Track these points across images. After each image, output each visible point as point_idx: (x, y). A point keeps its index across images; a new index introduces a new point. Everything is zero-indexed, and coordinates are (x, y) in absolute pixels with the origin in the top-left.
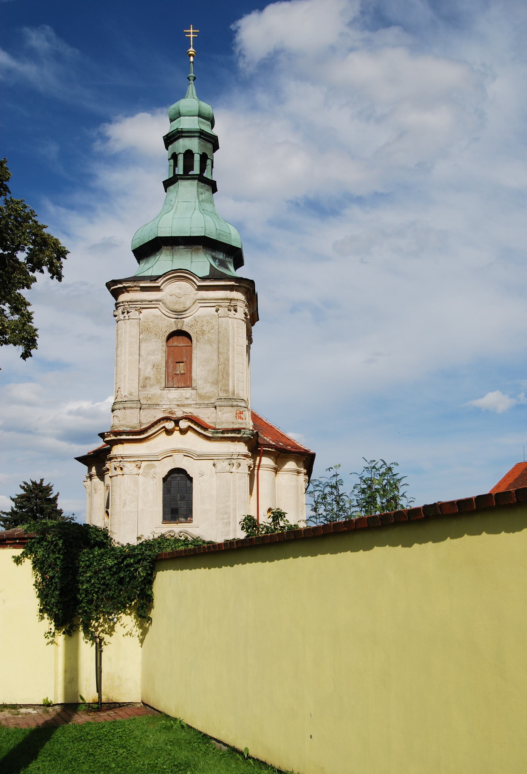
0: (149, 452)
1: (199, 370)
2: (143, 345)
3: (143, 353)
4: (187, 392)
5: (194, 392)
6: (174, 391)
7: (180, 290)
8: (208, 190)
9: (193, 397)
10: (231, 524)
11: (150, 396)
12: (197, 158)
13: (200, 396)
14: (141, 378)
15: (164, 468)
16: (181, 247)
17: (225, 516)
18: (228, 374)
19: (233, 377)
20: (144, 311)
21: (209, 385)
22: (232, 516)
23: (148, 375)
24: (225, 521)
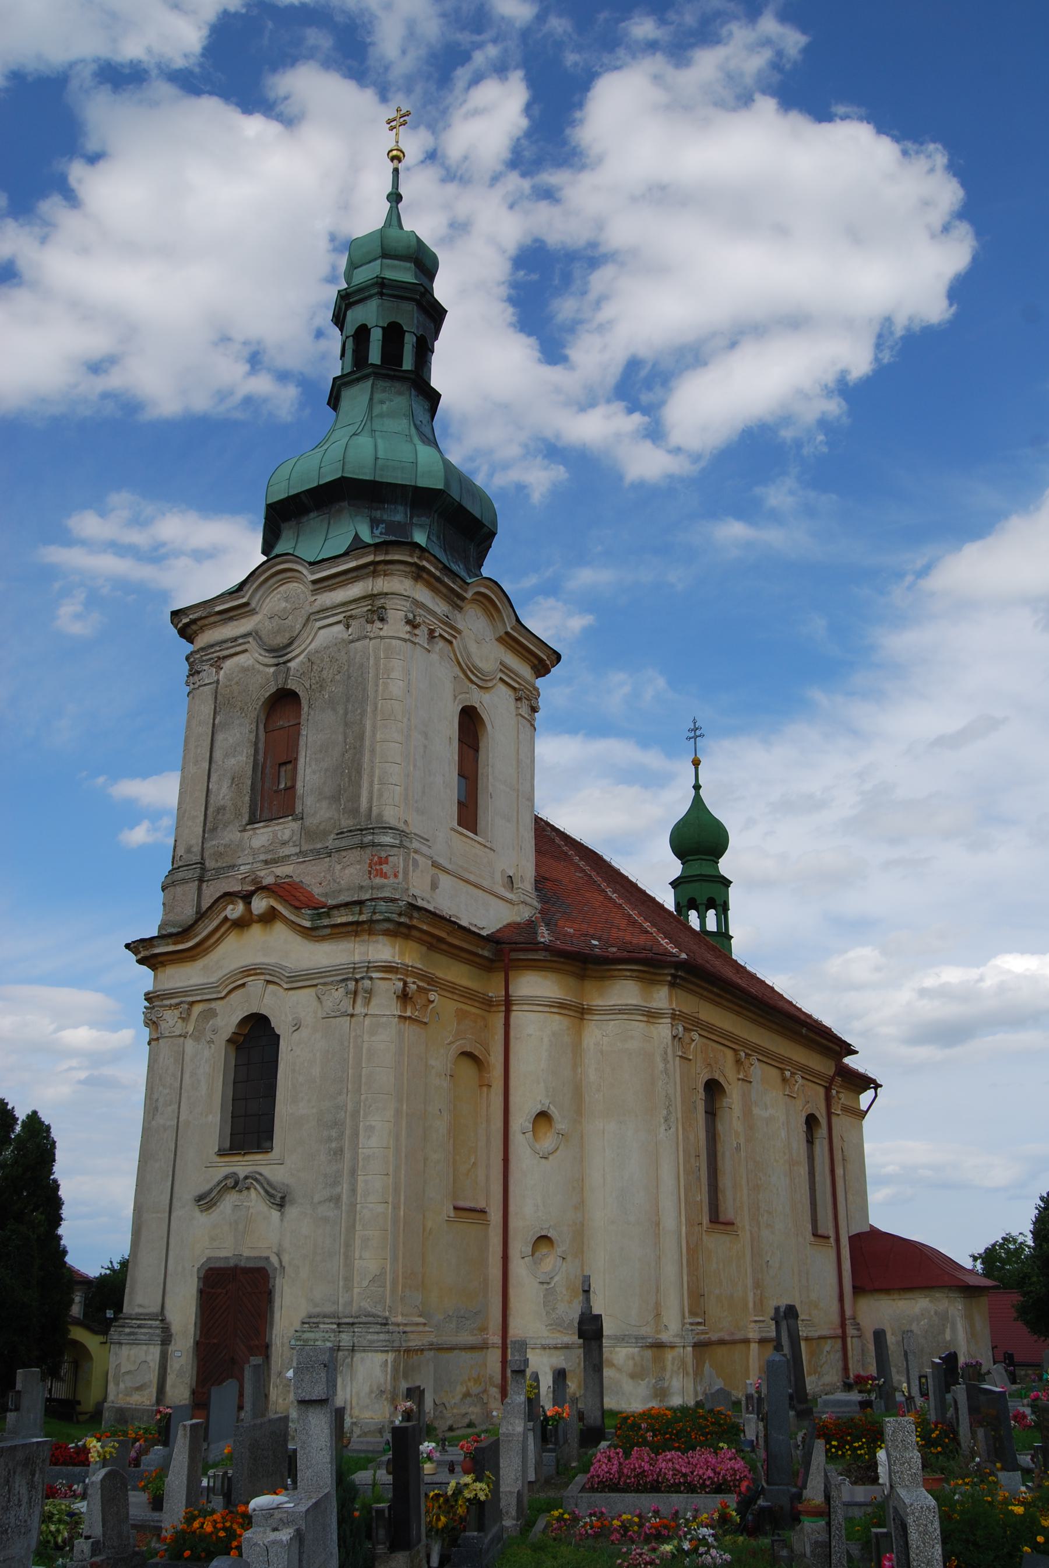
0: (205, 981)
1: (311, 775)
2: (220, 737)
3: (218, 754)
4: (286, 829)
5: (295, 825)
6: (262, 830)
7: (287, 601)
8: (400, 393)
9: (294, 838)
10: (347, 1155)
11: (221, 849)
12: (376, 336)
13: (309, 834)
14: (211, 810)
15: (229, 1018)
16: (312, 515)
17: (334, 1133)
18: (359, 772)
19: (372, 776)
20: (228, 664)
21: (325, 804)
22: (348, 1132)
23: (222, 803)
24: (334, 1145)
